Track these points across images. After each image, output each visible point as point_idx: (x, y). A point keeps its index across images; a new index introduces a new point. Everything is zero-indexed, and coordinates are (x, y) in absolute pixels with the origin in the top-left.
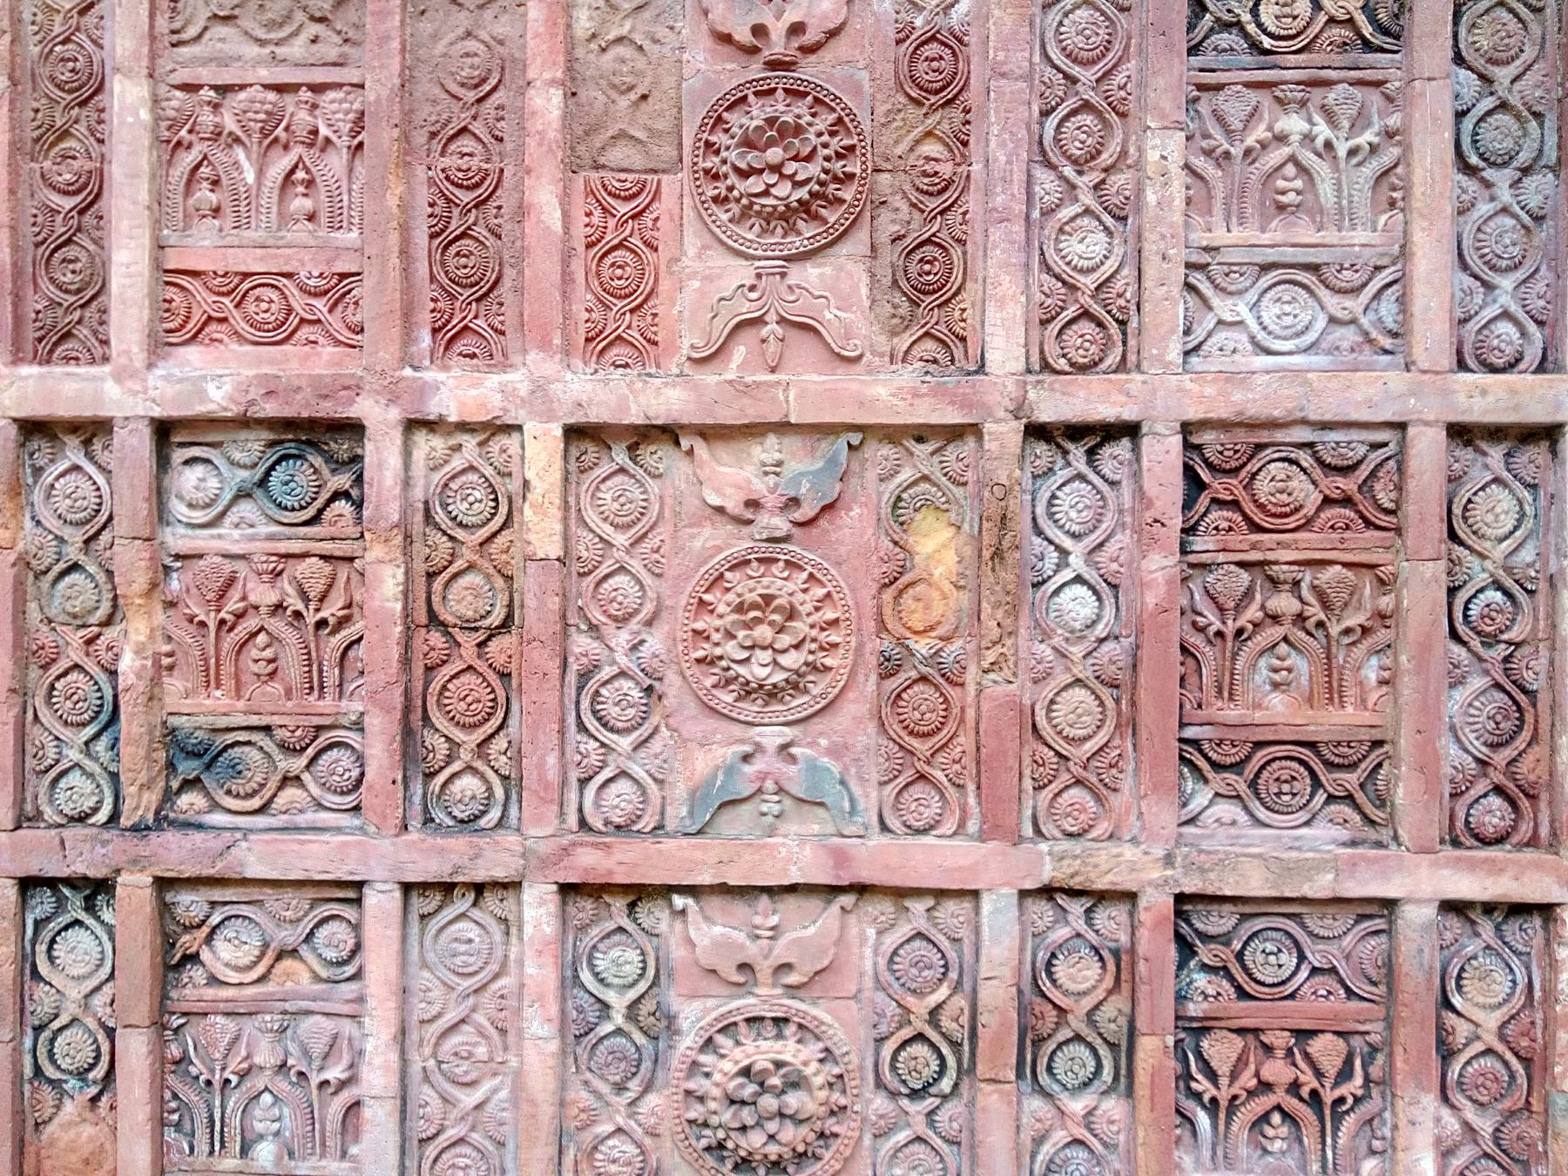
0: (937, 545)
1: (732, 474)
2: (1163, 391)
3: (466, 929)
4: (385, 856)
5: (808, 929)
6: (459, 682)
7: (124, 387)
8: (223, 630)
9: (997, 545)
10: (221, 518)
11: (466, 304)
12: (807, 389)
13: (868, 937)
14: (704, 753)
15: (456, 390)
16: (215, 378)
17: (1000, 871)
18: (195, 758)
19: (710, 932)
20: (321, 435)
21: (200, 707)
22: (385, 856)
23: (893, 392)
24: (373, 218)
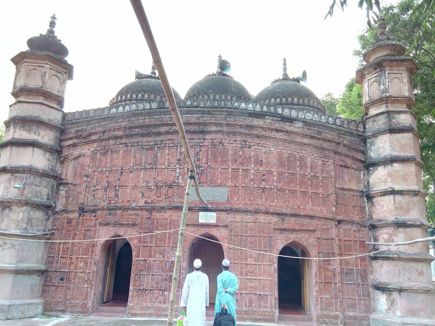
0: (164, 264)
1: (158, 262)
2: (170, 260)
3: (149, 276)
4: (146, 274)
5: (159, 276)
6: (149, 268)
7: (140, 259)
8: (142, 266)
9: (165, 264)
10: (142, 263)
11: (150, 256)
12: (160, 259)
13: (161, 276)
14: (156, 271)
15: (150, 259)
16: (143, 259)
17: (165, 274)
18: (141, 270)
19: (156, 276)
20: (146, 260)
21: (141, 269)
22: (146, 274)
23: (162, 260)
24: (147, 254)
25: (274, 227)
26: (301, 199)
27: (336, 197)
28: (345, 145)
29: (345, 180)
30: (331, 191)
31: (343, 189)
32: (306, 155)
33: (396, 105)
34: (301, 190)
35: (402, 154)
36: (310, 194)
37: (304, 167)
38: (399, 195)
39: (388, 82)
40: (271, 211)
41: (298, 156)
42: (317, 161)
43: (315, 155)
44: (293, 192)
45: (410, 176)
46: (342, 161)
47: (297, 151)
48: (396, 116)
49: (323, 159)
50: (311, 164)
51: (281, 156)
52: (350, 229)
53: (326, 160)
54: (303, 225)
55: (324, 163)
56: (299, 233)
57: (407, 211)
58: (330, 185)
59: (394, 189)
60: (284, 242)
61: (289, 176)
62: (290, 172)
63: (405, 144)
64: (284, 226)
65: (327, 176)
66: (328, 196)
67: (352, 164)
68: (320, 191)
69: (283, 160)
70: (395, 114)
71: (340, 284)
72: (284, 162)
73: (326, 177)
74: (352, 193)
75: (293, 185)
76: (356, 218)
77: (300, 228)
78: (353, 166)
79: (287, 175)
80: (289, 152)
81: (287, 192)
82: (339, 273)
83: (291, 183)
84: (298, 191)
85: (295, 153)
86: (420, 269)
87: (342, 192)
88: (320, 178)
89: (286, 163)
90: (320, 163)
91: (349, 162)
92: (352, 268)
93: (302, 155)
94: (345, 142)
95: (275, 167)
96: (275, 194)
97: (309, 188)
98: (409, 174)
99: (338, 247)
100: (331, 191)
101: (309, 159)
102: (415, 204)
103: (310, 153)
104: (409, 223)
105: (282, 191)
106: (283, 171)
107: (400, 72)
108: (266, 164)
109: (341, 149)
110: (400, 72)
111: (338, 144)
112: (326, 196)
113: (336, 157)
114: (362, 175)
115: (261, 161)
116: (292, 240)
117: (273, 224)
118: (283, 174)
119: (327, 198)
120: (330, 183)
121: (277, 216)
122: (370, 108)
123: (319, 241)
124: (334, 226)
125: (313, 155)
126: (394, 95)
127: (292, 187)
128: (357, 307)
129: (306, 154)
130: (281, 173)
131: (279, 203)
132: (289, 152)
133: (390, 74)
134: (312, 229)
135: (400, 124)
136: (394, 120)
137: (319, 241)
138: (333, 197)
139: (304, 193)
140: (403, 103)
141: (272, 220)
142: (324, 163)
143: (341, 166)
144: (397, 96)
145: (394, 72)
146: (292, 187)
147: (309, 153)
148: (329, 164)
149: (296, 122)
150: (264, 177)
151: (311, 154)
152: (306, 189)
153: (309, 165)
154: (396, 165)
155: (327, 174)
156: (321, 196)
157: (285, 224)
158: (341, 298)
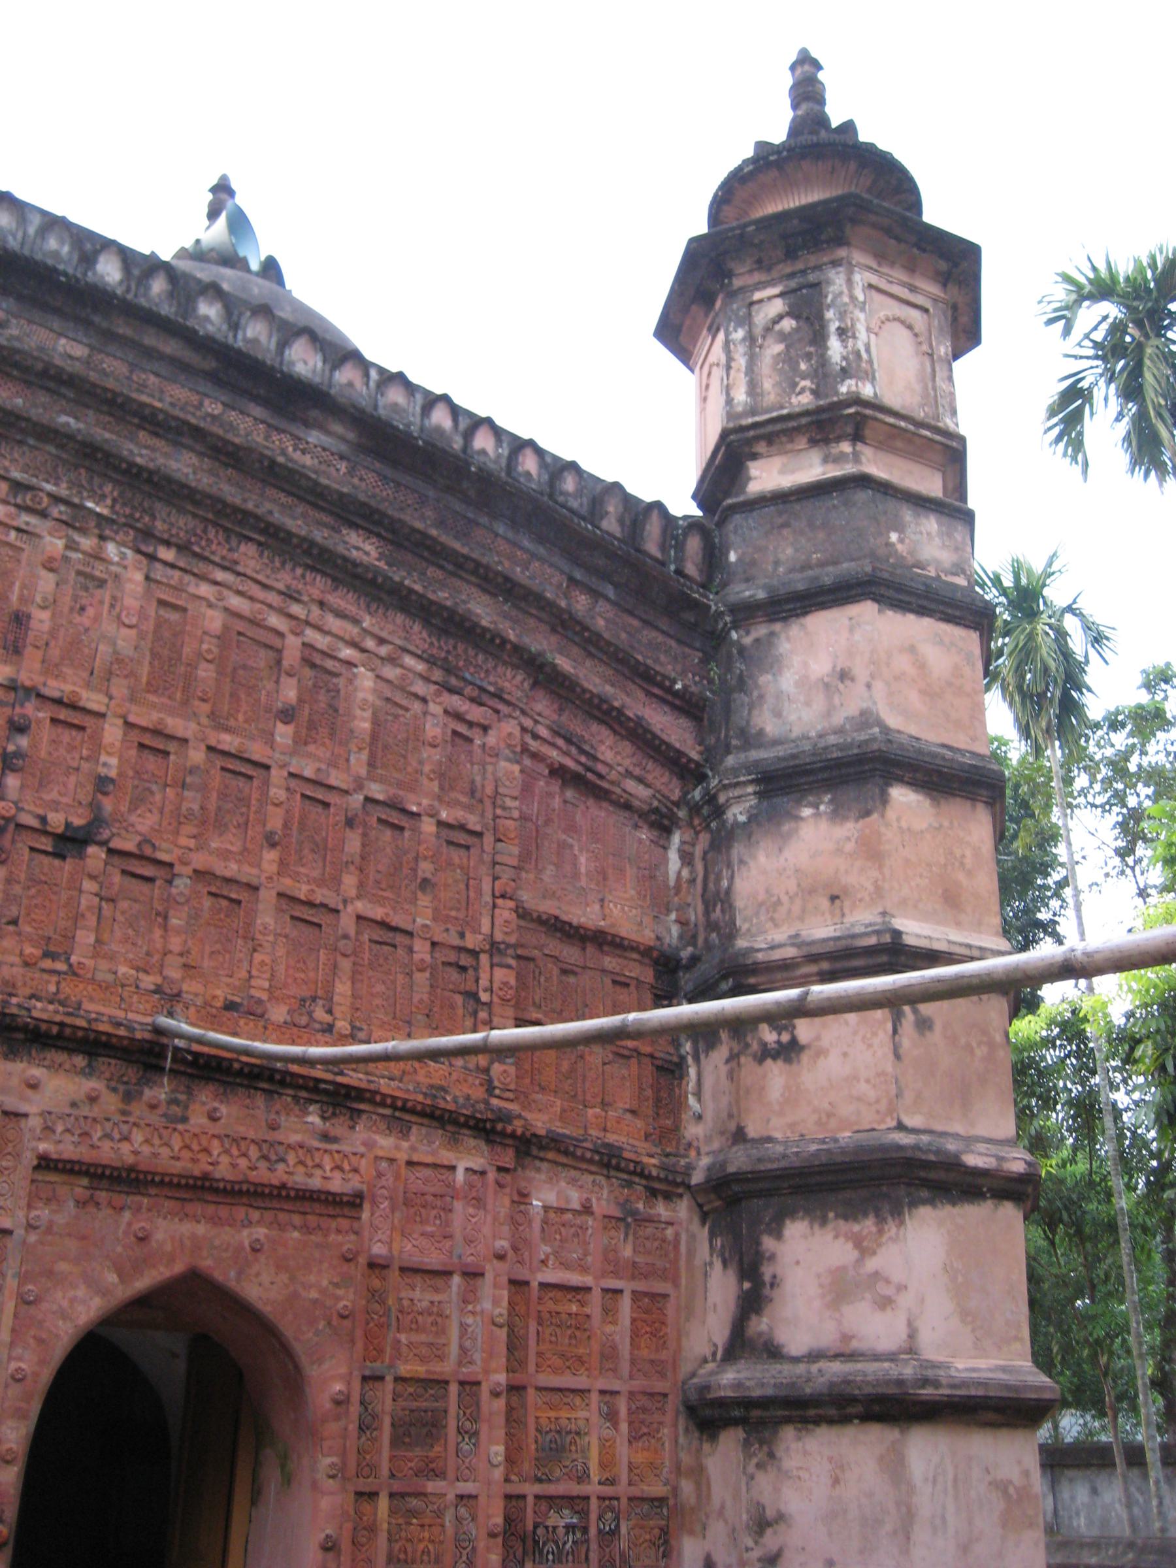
25: (43, 1147)
26: (281, 952)
29: (576, 875)
30: (486, 928)
32: (347, 653)
34: (286, 884)
36: (347, 922)
37: (324, 731)
40: (41, 1010)
41: (292, 644)
42: (417, 706)
43: (409, 661)
44: (231, 895)
45: (970, 873)
47: (296, 609)
49: (455, 702)
50: (376, 722)
51: (174, 616)
52: (587, 1209)
53: (476, 713)
54: (271, 1152)
55: (462, 729)
56: (241, 1212)
58: (486, 887)
59: (897, 934)
60: (112, 1278)
61: (216, 773)
62: (228, 741)
64: (125, 1148)
65: (473, 822)
66: (465, 960)
67: (629, 774)
68: (421, 915)
69: (187, 650)
72: (193, 666)
73: (462, 827)
74: (610, 962)
75: (231, 841)
76: (629, 1137)
77: (253, 1176)
78: (631, 785)
79: (197, 755)
80: (235, 602)
81: (182, 885)
82: (492, 1535)
83: (220, 826)
84: (267, 896)
85: (274, 620)
88: (428, 826)
89: (206, 672)
90: (433, 729)
93: (321, 641)
95: (120, 688)
96: (89, 886)
97: (349, 881)
98: (968, 861)
100: (486, 928)
101: (365, 680)
103: (382, 641)
105: (148, 871)
106: (176, 725)
108: (55, 653)
112: (452, 957)
114: (673, 857)
115: (20, 620)
116: (179, 1268)
117: (35, 1122)
118: (172, 747)
119: (454, 975)
120: (484, 870)
121: (80, 1061)
122: (755, 456)
123: (376, 1283)
124: (492, 1175)
125: (391, 660)
127: (222, 854)
129: (354, 644)
130: (159, 744)
131: (111, 957)
132: (235, 602)
133: (874, 293)
134: (337, 1185)
137: (376, 1283)
139: (307, 914)
141: (34, 1086)
142: (462, 729)
143: (558, 772)
146: (225, 855)
147: (370, 644)
148: (491, 739)
149: (314, 414)
150: (23, 742)
151: (383, 651)
152: (321, 882)
153: (363, 725)
155: (469, 808)
156: (421, 950)
157: (138, 1137)
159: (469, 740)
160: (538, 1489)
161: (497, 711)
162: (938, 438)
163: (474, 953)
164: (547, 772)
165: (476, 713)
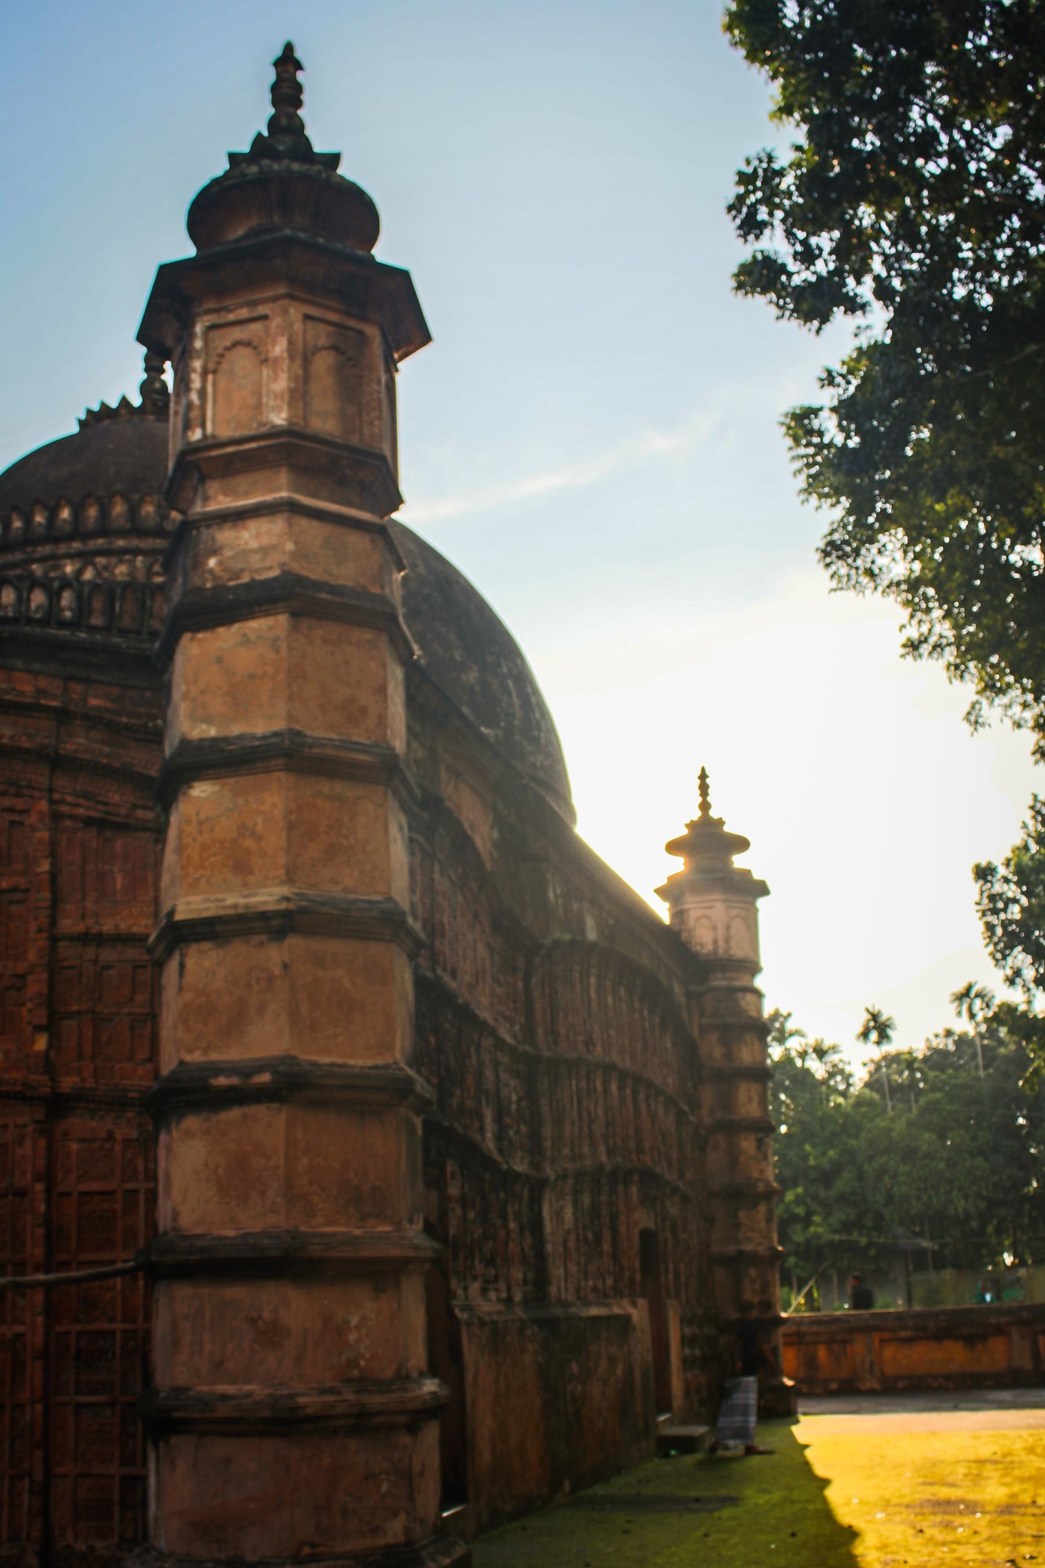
27: (51, 983)
28: (93, 721)
31: (100, 940)
33: (242, 481)
35: (236, 730)
38: (206, 945)
39: (204, 374)
46: (86, 796)
48: (225, 535)
52: (111, 1137)
53: (20, 803)
55: (16, 817)
57: (236, 1023)
63: (252, 677)
65: (22, 881)
67: (134, 807)
70: (208, 527)
71: (39, 1407)
78: (140, 813)
86: (267, 1315)
87: (90, 952)
91: (116, 798)
92: (106, 1326)
94: (93, 702)
98: (260, 829)
99: (40, 1231)
102: (271, 979)
104: (222, 1081)
107: (262, 310)
109: (79, 742)
110: (262, 310)
111: (63, 716)
113: (61, 781)
126: (226, 432)
128: (117, 1517)
135: (237, 576)
136: (212, 562)
138: (37, 985)
140: (274, 466)
142: (16, 817)
143: (89, 822)
144: (238, 434)
145: (231, 317)
154: (201, 790)
158: (39, 1476)
159: (21, 824)
160: (78, 1327)
161: (32, 797)
162: (262, 443)
163: (23, 976)
164: (81, 825)
165: (20, 803)
